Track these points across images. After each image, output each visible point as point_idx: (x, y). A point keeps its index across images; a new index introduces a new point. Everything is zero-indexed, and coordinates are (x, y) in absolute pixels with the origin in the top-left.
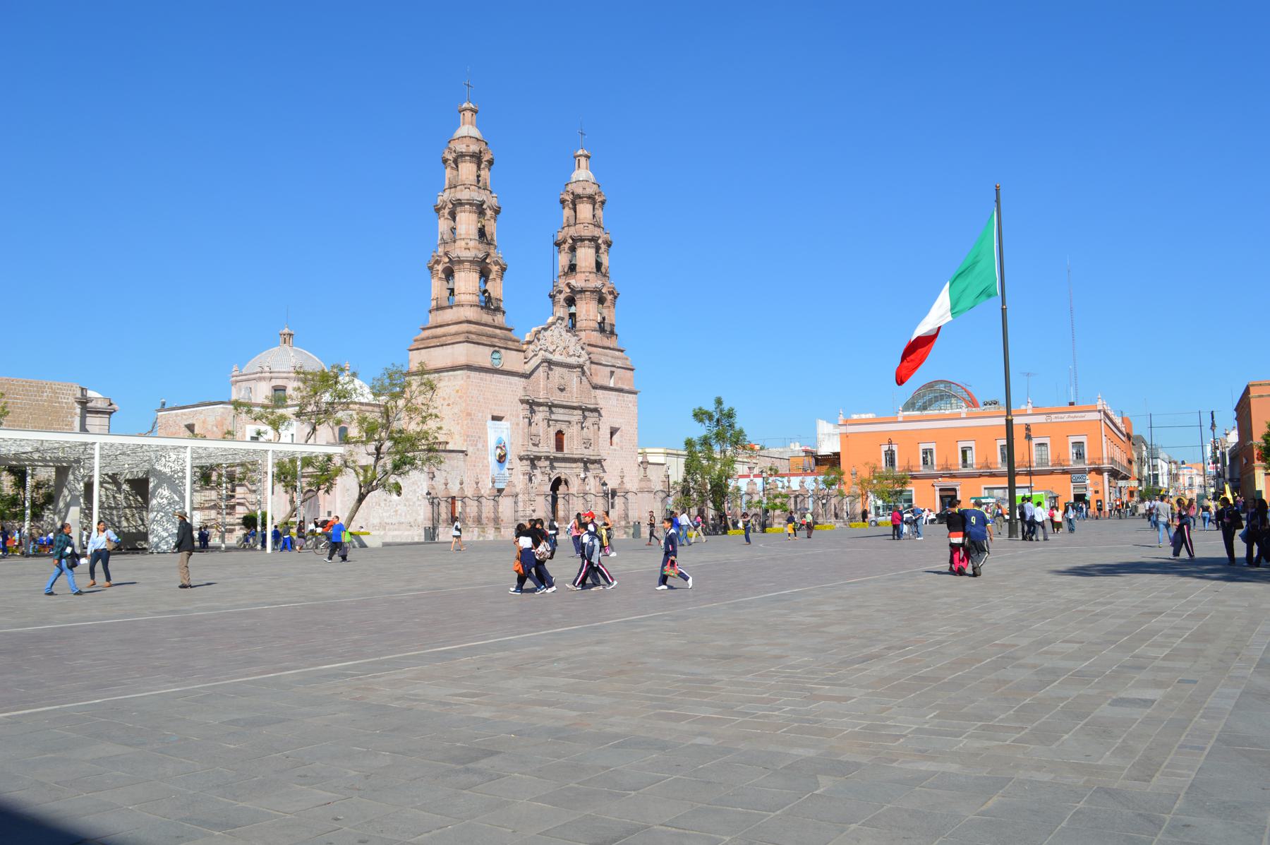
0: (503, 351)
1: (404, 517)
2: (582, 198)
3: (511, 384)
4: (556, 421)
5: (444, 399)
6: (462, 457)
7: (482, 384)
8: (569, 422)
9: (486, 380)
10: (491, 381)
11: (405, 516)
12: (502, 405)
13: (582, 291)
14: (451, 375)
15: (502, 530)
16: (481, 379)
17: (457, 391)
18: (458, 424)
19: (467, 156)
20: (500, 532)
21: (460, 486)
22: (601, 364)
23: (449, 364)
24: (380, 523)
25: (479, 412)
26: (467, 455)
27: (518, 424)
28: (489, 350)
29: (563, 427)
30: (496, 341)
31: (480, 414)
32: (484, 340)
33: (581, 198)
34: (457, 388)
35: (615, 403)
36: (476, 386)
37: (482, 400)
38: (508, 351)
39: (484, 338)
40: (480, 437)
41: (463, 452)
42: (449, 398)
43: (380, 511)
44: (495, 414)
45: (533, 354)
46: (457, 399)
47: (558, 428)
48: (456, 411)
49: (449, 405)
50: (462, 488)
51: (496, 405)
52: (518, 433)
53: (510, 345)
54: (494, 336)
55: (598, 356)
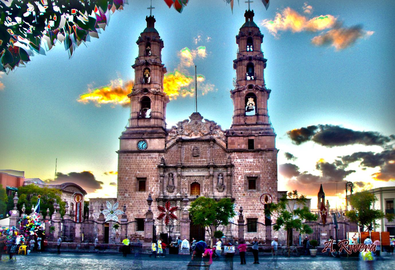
0: (148, 140)
4: (191, 176)
8: (204, 176)
12: (144, 171)
16: (129, 158)
25: (126, 176)
29: (198, 180)
31: (128, 177)
35: (252, 160)
36: (125, 162)
37: (129, 170)
38: (152, 140)
39: (135, 135)
40: (126, 190)
44: (138, 177)
45: (171, 138)
47: (193, 180)
51: (139, 171)
52: (157, 186)
53: (155, 136)
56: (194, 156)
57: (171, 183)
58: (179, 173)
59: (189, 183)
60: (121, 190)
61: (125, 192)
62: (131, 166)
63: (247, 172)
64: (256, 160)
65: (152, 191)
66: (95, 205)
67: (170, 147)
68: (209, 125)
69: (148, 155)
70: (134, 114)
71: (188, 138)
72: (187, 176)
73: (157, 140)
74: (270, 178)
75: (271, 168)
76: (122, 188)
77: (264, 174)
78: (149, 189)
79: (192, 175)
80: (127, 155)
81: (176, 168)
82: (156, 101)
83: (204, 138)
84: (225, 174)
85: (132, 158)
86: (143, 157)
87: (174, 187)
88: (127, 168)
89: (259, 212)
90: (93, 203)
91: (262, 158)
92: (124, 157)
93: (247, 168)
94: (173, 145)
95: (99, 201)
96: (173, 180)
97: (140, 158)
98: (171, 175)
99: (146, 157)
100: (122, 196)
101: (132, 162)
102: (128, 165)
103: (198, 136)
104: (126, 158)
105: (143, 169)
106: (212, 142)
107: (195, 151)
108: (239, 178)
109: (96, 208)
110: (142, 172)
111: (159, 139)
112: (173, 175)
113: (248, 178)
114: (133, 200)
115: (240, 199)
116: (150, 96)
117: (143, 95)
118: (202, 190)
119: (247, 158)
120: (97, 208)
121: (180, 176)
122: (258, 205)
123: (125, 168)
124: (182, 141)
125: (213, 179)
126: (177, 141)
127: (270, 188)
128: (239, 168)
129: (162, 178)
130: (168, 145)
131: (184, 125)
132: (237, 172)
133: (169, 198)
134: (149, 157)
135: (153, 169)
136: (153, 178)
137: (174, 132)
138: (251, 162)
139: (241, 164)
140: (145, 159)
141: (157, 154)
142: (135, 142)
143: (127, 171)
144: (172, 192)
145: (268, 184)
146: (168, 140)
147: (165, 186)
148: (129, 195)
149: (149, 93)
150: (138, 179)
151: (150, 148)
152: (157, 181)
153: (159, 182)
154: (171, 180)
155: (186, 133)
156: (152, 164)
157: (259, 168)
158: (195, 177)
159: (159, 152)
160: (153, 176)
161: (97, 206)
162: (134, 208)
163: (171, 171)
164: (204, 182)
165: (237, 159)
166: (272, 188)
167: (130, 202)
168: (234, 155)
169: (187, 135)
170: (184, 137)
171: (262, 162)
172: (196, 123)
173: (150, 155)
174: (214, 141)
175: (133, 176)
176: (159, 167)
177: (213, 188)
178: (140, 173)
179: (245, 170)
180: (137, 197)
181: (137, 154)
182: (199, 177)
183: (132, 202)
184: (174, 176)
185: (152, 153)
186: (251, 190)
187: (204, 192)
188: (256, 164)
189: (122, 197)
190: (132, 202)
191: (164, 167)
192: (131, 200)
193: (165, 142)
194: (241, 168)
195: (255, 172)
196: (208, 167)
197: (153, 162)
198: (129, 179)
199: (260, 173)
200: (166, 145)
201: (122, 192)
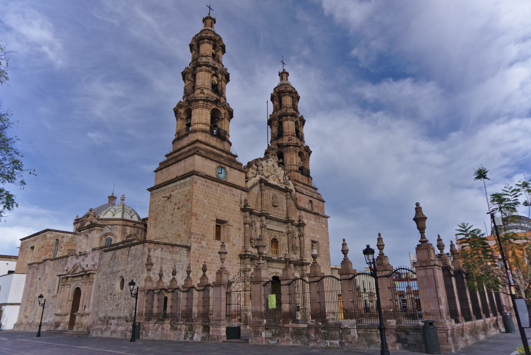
0: (228, 168)
1: (122, 312)
2: (285, 92)
3: (234, 195)
4: (271, 230)
5: (176, 204)
6: (185, 252)
7: (208, 191)
9: (211, 188)
10: (216, 190)
11: (124, 309)
13: (288, 146)
14: (182, 184)
15: (211, 329)
16: (208, 186)
17: (186, 196)
18: (185, 223)
19: (206, 39)
20: (209, 331)
21: (172, 277)
22: (303, 194)
23: (181, 173)
24: (105, 317)
25: (204, 213)
26: (190, 250)
27: (240, 229)
30: (222, 160)
31: (205, 216)
32: (212, 156)
33: (284, 93)
34: (186, 193)
35: (313, 223)
37: (207, 204)
38: (232, 169)
40: (204, 236)
41: (186, 247)
42: (179, 203)
43: (107, 305)
44: (219, 218)
46: (186, 202)
48: (184, 212)
49: (179, 208)
50: (174, 279)
51: (220, 210)
52: (239, 236)
54: (222, 157)
55: (301, 189)
59: (270, 238)
61: (201, 239)
62: (209, 200)
63: (311, 234)
65: (235, 243)
66: (156, 255)
69: (230, 190)
70: (203, 125)
73: (237, 172)
74: (325, 245)
75: (325, 234)
76: (198, 231)
78: (231, 239)
80: (206, 182)
83: (279, 185)
84: (297, 234)
86: (225, 191)
88: (205, 201)
90: (152, 250)
91: (319, 222)
92: (201, 183)
93: (311, 231)
94: (254, 185)
95: (162, 249)
97: (220, 189)
99: (228, 191)
100: (198, 244)
101: (212, 194)
102: (207, 196)
103: (275, 183)
104: (204, 185)
105: (225, 207)
108: (307, 241)
109: (157, 261)
110: (223, 211)
111: (240, 172)
113: (312, 241)
114: (212, 252)
119: (310, 220)
120: (159, 260)
123: (203, 201)
127: (326, 256)
128: (306, 230)
130: (250, 184)
134: (231, 193)
135: (235, 211)
136: (236, 224)
138: (313, 225)
140: (227, 194)
141: (239, 191)
142: (214, 165)
143: (205, 205)
148: (207, 244)
151: (230, 180)
153: (242, 230)
156: (234, 204)
158: (275, 232)
160: (236, 222)
161: (160, 257)
162: (213, 265)
163: (255, 218)
164: (283, 240)
166: (327, 255)
167: (208, 255)
173: (232, 191)
175: (212, 214)
178: (221, 212)
180: (217, 248)
181: (217, 184)
182: (278, 233)
183: (211, 256)
184: (257, 226)
185: (234, 189)
188: (316, 228)
189: (198, 246)
190: (211, 256)
192: (209, 252)
193: (246, 178)
194: (307, 230)
195: (316, 235)
197: (235, 201)
198: (207, 218)
200: (246, 182)
201: (198, 238)
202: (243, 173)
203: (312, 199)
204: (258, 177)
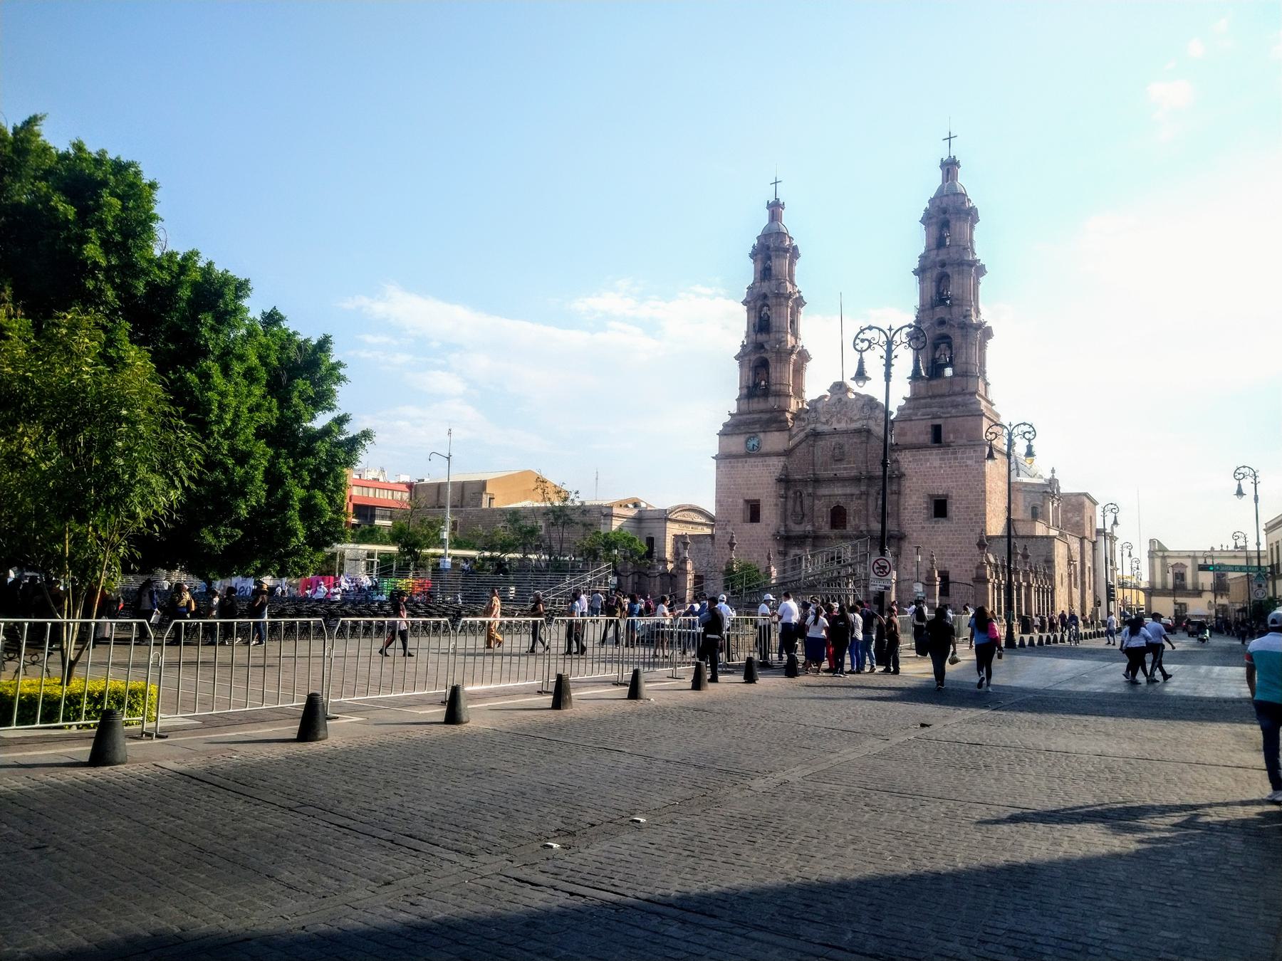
0: (761, 435)
8: (852, 495)
16: (732, 467)
25: (729, 497)
28: (742, 439)
29: (842, 501)
35: (937, 463)
40: (729, 521)
51: (748, 489)
56: (837, 460)
57: (798, 509)
58: (810, 490)
60: (720, 521)
64: (945, 464)
67: (797, 445)
68: (860, 403)
71: (826, 428)
72: (824, 496)
77: (961, 489)
79: (832, 493)
80: (730, 463)
81: (805, 482)
82: (779, 365)
85: (737, 467)
87: (803, 515)
89: (951, 560)
96: (801, 502)
98: (798, 494)
105: (755, 484)
106: (864, 434)
107: (837, 451)
108: (914, 498)
112: (801, 495)
113: (929, 495)
115: (915, 534)
116: (770, 356)
117: (758, 355)
118: (849, 520)
119: (928, 460)
121: (813, 496)
122: (948, 547)
124: (816, 435)
125: (867, 500)
126: (807, 436)
128: (914, 479)
129: (782, 500)
131: (820, 406)
132: (909, 487)
133: (794, 534)
137: (803, 420)
139: (916, 472)
144: (801, 523)
145: (967, 508)
146: (794, 433)
147: (789, 513)
149: (766, 351)
150: (747, 501)
152: (776, 505)
154: (798, 503)
155: (824, 420)
157: (951, 478)
159: (778, 454)
164: (852, 507)
165: (910, 462)
168: (905, 455)
169: (824, 424)
170: (820, 428)
171: (956, 467)
172: (840, 400)
174: (869, 431)
176: (779, 480)
177: (867, 516)
179: (925, 483)
181: (744, 460)
186: (936, 519)
187: (853, 523)
191: (785, 481)
196: (857, 480)
198: (732, 502)
199: (953, 488)
202: (784, 433)
203: (938, 422)
204: (808, 429)
